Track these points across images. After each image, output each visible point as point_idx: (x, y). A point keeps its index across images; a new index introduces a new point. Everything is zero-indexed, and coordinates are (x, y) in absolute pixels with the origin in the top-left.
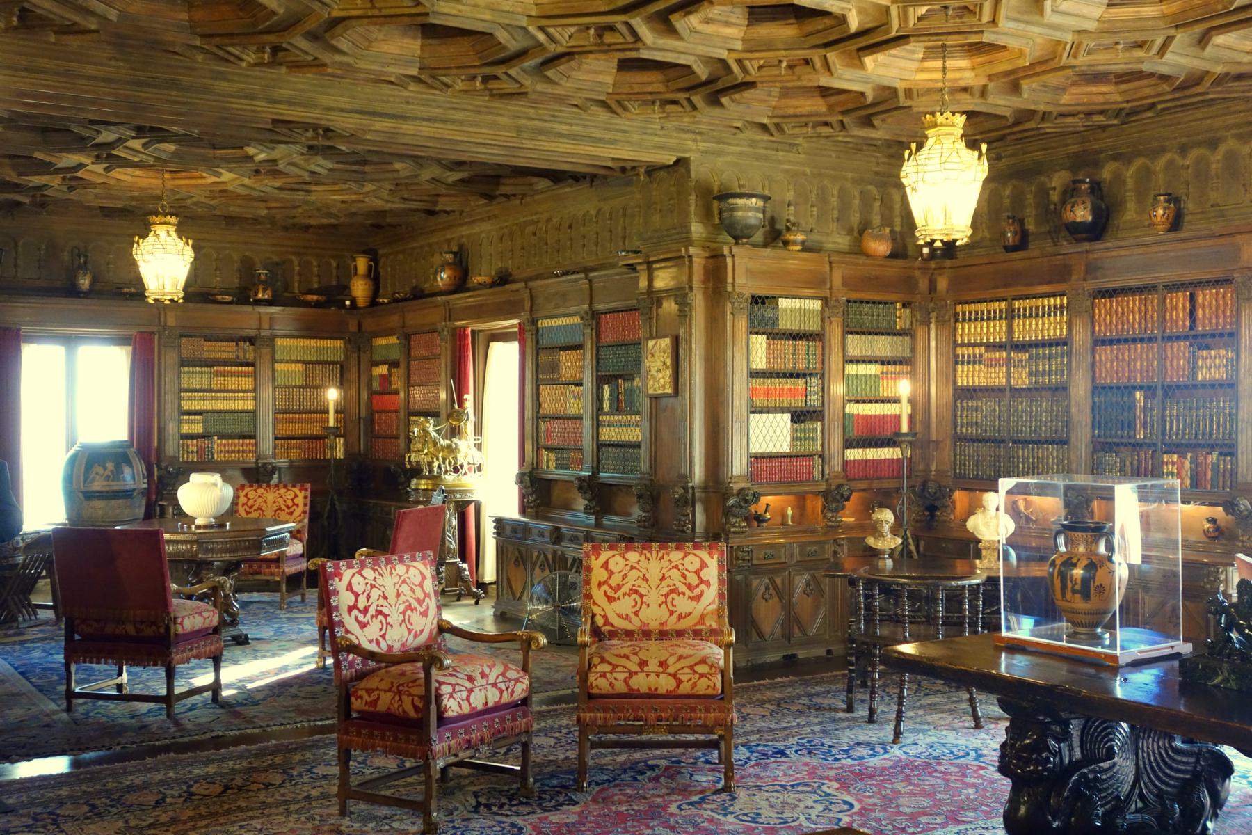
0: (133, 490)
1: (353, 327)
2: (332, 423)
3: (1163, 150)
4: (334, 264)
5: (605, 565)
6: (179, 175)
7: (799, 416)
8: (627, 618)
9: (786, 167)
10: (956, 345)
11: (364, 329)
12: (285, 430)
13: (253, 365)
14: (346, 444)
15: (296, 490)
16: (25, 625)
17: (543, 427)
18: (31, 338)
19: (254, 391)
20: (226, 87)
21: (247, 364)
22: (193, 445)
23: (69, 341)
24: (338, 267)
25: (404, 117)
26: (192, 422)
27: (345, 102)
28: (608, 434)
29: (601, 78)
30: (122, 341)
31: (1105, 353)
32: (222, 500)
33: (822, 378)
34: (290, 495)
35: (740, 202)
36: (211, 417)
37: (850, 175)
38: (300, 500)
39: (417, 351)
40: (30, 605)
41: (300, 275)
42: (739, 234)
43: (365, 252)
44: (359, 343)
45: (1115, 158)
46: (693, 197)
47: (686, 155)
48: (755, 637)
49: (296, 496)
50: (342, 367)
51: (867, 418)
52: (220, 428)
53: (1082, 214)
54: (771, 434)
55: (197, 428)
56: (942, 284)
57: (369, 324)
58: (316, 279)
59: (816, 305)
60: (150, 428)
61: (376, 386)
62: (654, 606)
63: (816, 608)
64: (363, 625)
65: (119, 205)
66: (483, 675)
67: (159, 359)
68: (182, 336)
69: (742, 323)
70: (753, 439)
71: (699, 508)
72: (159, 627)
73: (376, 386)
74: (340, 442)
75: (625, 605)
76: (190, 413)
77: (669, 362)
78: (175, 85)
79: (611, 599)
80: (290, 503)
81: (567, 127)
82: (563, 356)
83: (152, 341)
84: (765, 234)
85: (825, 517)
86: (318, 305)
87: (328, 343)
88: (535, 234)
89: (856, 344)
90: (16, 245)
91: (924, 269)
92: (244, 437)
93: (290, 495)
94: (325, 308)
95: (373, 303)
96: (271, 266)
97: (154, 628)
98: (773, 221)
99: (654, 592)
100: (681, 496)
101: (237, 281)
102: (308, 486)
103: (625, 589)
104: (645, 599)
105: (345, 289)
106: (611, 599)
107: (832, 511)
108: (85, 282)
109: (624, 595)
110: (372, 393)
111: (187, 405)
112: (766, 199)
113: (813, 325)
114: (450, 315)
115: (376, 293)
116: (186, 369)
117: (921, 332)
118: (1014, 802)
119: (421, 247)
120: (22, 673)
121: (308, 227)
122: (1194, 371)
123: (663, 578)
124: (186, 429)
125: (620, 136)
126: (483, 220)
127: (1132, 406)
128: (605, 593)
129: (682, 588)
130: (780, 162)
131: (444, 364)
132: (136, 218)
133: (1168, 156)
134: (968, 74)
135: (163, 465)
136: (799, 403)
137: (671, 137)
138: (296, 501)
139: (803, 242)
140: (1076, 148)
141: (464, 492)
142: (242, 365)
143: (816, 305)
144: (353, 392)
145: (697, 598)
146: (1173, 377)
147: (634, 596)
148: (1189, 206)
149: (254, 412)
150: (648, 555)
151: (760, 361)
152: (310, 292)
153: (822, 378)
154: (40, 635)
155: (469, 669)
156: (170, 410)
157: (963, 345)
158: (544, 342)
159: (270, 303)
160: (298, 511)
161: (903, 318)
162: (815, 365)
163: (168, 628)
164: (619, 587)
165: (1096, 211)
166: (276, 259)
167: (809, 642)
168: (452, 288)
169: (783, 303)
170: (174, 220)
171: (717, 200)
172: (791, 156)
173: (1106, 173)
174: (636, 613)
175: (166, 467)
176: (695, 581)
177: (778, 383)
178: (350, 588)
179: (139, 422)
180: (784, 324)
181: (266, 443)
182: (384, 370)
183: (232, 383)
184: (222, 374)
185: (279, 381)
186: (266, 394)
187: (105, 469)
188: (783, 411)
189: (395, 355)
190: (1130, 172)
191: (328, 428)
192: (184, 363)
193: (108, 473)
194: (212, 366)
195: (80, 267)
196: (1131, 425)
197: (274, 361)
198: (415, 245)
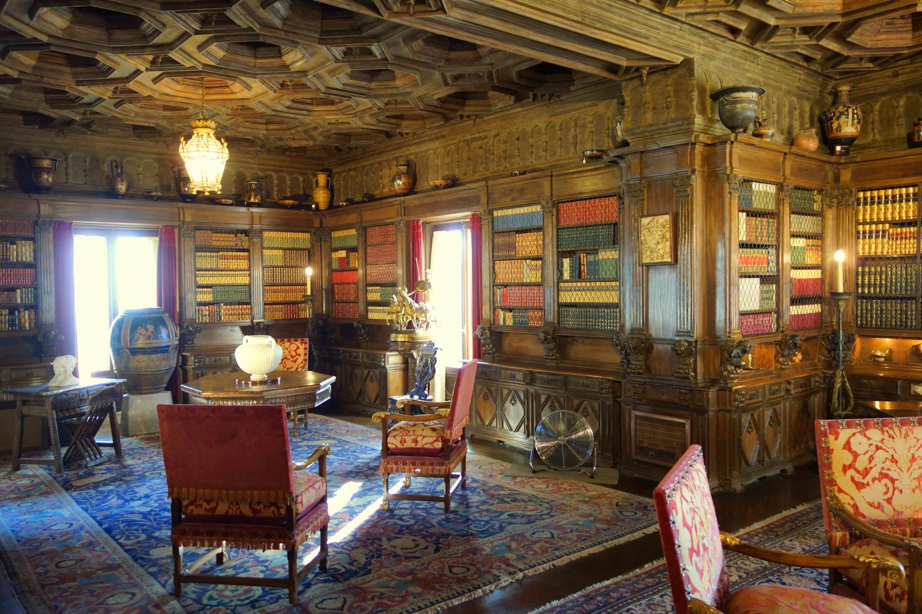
0: (168, 346)
1: (317, 224)
2: (309, 293)
4: (301, 179)
5: (847, 446)
6: (212, 91)
8: (879, 506)
9: (750, 75)
11: (324, 225)
12: (272, 297)
13: (247, 250)
15: (298, 343)
16: (93, 464)
17: (499, 292)
18: (80, 230)
19: (249, 269)
21: (244, 251)
22: (206, 310)
24: (304, 182)
26: (205, 293)
28: (568, 297)
30: (150, 233)
32: (275, 358)
33: (777, 250)
34: (293, 347)
36: (219, 289)
37: (784, 87)
38: (301, 351)
40: (93, 442)
41: (278, 186)
43: (323, 170)
44: (321, 235)
47: (691, 56)
48: (744, 466)
49: (298, 348)
50: (309, 252)
55: (208, 297)
56: (846, 176)
57: (329, 221)
58: (289, 190)
60: (174, 298)
61: (335, 266)
62: (907, 491)
63: (775, 435)
67: (179, 247)
68: (197, 229)
72: (278, 508)
73: (335, 266)
75: (876, 492)
76: (203, 287)
77: (668, 235)
79: (860, 486)
80: (294, 354)
81: (617, 18)
82: (519, 237)
83: (173, 234)
85: (777, 361)
87: (300, 235)
88: (481, 148)
90: (67, 158)
92: (243, 304)
93: (293, 347)
94: (296, 211)
95: (331, 206)
97: (273, 508)
99: (905, 475)
100: (687, 349)
101: (233, 190)
102: (307, 340)
103: (874, 473)
104: (897, 484)
106: (860, 486)
107: (783, 356)
108: (122, 187)
109: (874, 480)
110: (332, 271)
111: (201, 281)
112: (761, 92)
114: (406, 210)
116: (200, 254)
119: (372, 165)
120: (108, 531)
123: (913, 459)
124: (201, 298)
126: (431, 140)
128: (853, 479)
130: (746, 70)
135: (185, 325)
137: (683, 38)
138: (298, 351)
142: (240, 250)
143: (772, 189)
147: (885, 481)
150: (891, 432)
152: (285, 198)
153: (777, 250)
154: (108, 476)
157: (864, 223)
158: (499, 227)
159: (258, 205)
160: (301, 359)
163: (289, 510)
164: (866, 472)
166: (261, 174)
167: (773, 464)
168: (405, 191)
174: (889, 501)
175: (187, 327)
179: (165, 294)
182: (343, 254)
183: (233, 264)
184: (226, 258)
186: (258, 273)
187: (147, 330)
189: (353, 243)
192: (199, 249)
193: (149, 333)
194: (218, 252)
195: (118, 175)
197: (263, 248)
198: (366, 163)
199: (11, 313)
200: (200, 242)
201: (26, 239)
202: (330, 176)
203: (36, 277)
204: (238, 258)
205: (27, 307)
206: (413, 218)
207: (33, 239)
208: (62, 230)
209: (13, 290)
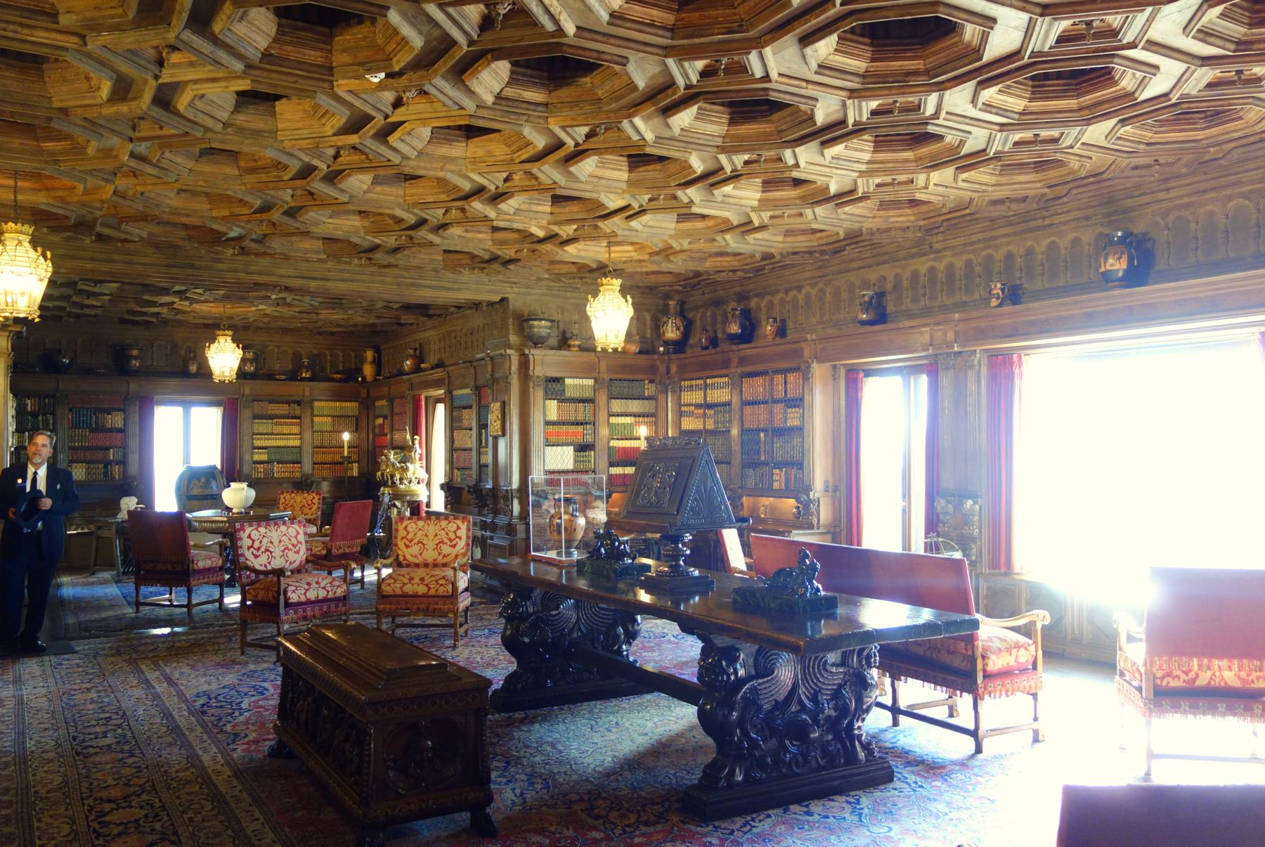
1: (364, 394)
3: (777, 292)
7: (582, 448)
10: (681, 406)
12: (319, 458)
14: (359, 467)
18: (161, 403)
20: (220, 266)
22: (261, 467)
23: (186, 405)
25: (328, 280)
27: (291, 272)
29: (434, 257)
31: (748, 409)
32: (247, 498)
35: (536, 323)
39: (397, 410)
42: (537, 342)
44: (367, 405)
45: (757, 295)
46: (511, 320)
51: (624, 449)
52: (278, 457)
53: (734, 328)
54: (562, 458)
55: (264, 457)
56: (674, 369)
59: (591, 382)
60: (234, 457)
61: (377, 430)
64: (256, 557)
65: (210, 322)
66: (317, 583)
69: (540, 393)
70: (547, 460)
71: (516, 502)
74: (355, 466)
75: (415, 550)
78: (192, 266)
79: (407, 547)
84: (559, 341)
86: (341, 380)
87: (348, 404)
89: (617, 405)
91: (663, 361)
94: (347, 382)
96: (312, 357)
98: (564, 333)
105: (359, 371)
106: (407, 547)
108: (193, 368)
110: (375, 436)
111: (257, 443)
113: (588, 394)
115: (378, 373)
117: (661, 398)
118: (505, 629)
121: (332, 334)
122: (786, 420)
124: (257, 458)
125: (463, 286)
127: (759, 442)
129: (446, 541)
131: (408, 418)
132: (210, 330)
133: (780, 295)
134: (633, 254)
136: (579, 439)
139: (579, 346)
140: (738, 289)
141: (412, 495)
144: (364, 435)
145: (454, 546)
146: (778, 423)
148: (790, 324)
149: (300, 447)
151: (553, 415)
152: (337, 373)
155: (309, 580)
156: (246, 446)
158: (456, 404)
159: (310, 380)
160: (315, 507)
161: (649, 389)
162: (589, 417)
164: (412, 540)
165: (742, 326)
166: (315, 352)
169: (568, 381)
170: (230, 333)
171: (523, 321)
172: (576, 295)
173: (753, 303)
176: (453, 536)
177: (564, 428)
178: (249, 536)
180: (568, 394)
181: (307, 467)
183: (286, 429)
185: (316, 428)
188: (567, 444)
189: (386, 411)
190: (764, 303)
191: (343, 457)
196: (759, 453)
199: (105, 467)
200: (257, 411)
201: (119, 410)
202: (377, 350)
203: (125, 440)
204: (290, 424)
205: (118, 463)
206: (416, 393)
207: (124, 411)
208: (146, 405)
209: (108, 449)
